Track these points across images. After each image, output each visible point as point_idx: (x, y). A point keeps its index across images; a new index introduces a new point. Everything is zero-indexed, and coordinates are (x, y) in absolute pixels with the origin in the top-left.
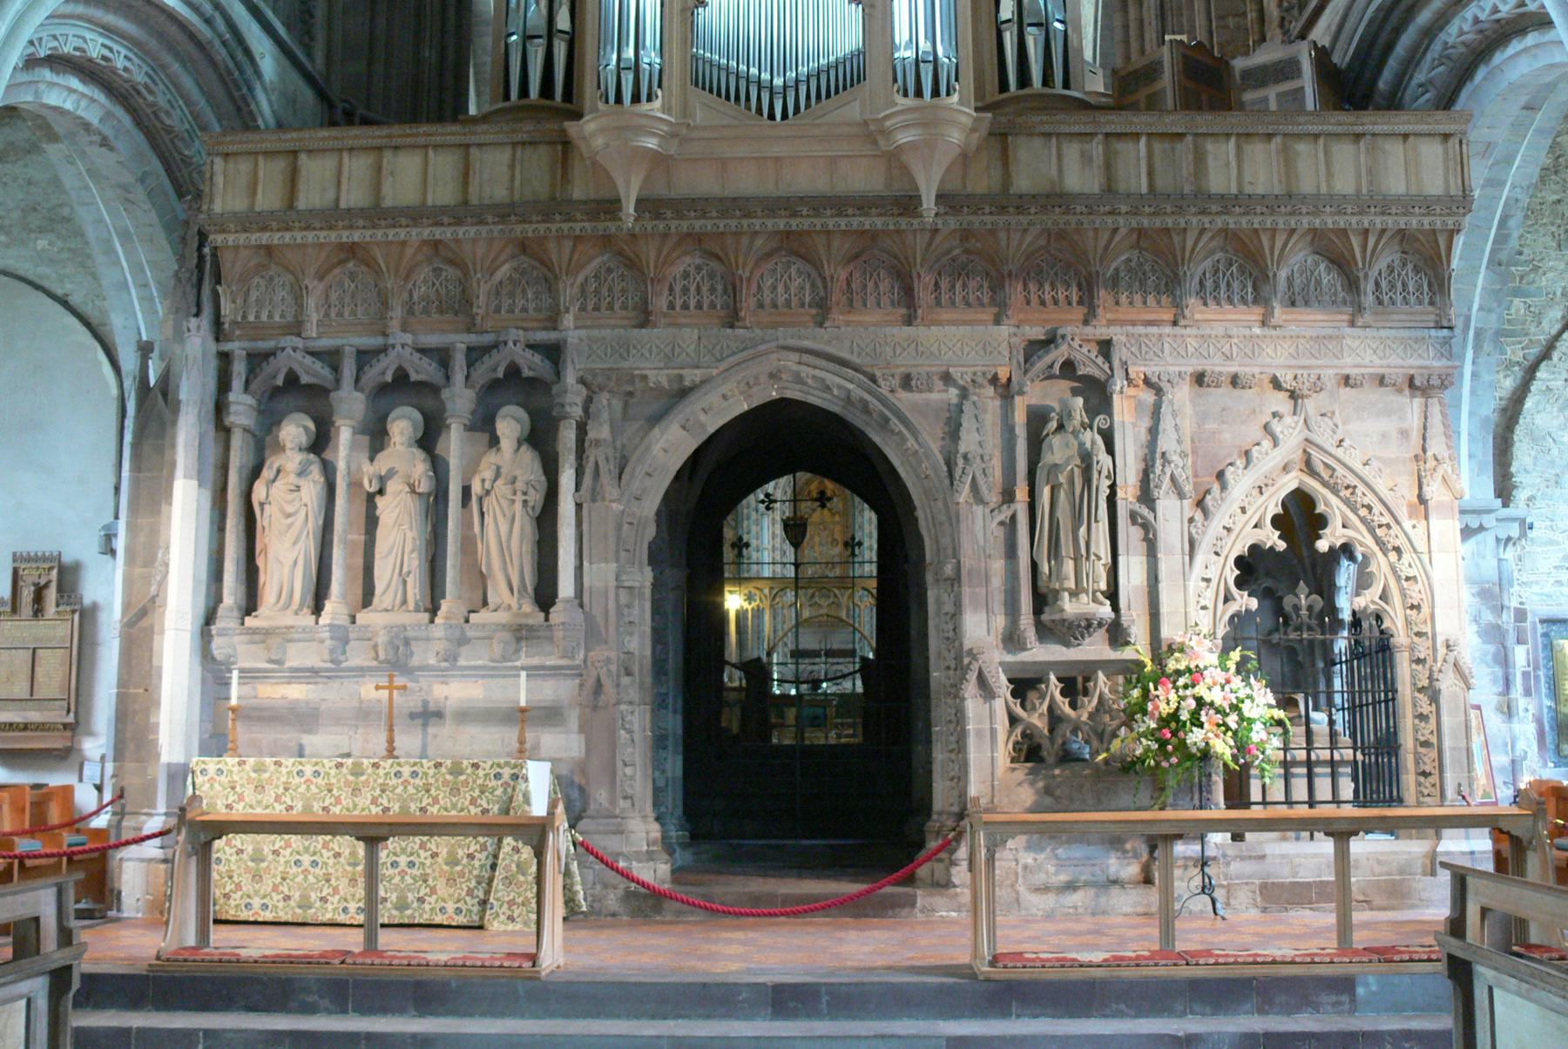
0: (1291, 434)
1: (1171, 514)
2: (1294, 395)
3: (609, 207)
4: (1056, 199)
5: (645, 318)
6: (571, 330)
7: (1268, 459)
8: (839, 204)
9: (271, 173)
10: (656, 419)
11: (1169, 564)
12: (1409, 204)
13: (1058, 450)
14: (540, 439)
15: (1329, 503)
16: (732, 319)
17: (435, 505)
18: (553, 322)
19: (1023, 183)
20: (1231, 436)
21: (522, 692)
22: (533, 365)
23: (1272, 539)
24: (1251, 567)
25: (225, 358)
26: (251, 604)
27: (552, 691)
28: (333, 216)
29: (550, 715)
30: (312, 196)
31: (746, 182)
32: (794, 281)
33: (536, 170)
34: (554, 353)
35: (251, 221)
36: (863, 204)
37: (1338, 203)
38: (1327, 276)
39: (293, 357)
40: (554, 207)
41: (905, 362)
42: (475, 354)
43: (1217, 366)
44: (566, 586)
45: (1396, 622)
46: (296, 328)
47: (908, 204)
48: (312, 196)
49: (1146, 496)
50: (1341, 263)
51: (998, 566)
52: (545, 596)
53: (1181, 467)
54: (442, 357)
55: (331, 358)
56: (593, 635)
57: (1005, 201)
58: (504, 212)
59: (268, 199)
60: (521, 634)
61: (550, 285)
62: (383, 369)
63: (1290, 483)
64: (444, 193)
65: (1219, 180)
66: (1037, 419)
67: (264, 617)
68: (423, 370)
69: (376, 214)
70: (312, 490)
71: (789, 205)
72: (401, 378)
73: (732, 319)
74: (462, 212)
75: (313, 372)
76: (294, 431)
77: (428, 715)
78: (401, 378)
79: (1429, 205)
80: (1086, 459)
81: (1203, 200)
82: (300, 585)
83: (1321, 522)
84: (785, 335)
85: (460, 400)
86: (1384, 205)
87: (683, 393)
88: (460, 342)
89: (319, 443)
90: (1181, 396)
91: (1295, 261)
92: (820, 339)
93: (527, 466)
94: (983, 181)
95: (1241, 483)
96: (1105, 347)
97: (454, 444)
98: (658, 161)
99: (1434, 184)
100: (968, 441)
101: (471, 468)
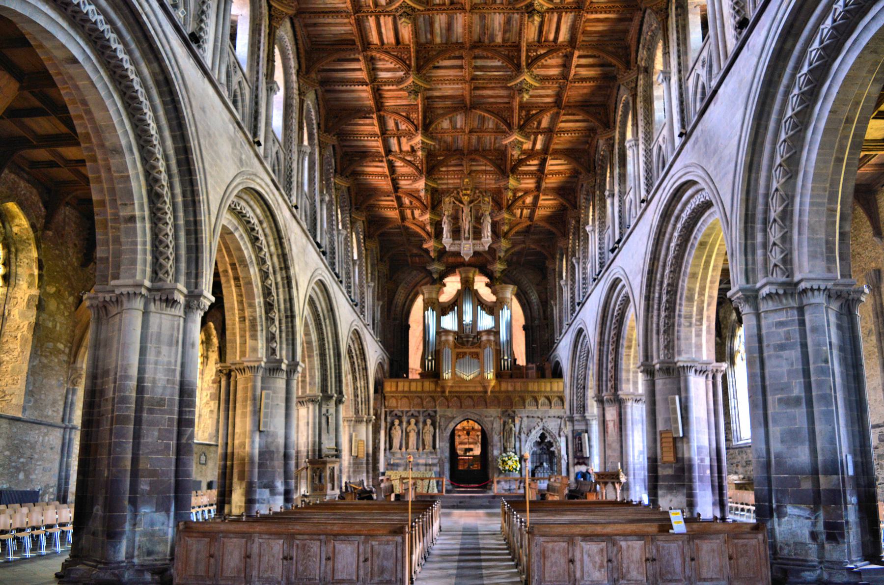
0: (541, 425)
1: (523, 436)
2: (542, 419)
3: (443, 392)
4: (507, 391)
5: (448, 407)
6: (438, 409)
7: (538, 429)
8: (476, 392)
9: (394, 384)
10: (450, 422)
11: (523, 443)
12: (558, 392)
13: (507, 427)
14: (433, 424)
15: (547, 435)
16: (461, 407)
17: (418, 434)
18: (435, 407)
19: (503, 389)
20: (532, 425)
21: (430, 462)
22: (432, 414)
23: (539, 440)
24: (538, 444)
25: (386, 412)
26: (391, 448)
27: (436, 461)
28: (403, 392)
29: (434, 465)
30: (400, 389)
31: (463, 389)
32: (470, 402)
33: (432, 387)
34: (435, 412)
35: (391, 392)
36: (480, 392)
37: (547, 392)
38: (547, 401)
39: (396, 412)
40: (435, 391)
41: (486, 414)
42: (424, 412)
43: (531, 415)
44: (437, 446)
45: (556, 452)
46: (397, 407)
47: (486, 392)
48: (400, 389)
49: (520, 433)
50: (548, 398)
51: (499, 444)
52: (434, 447)
53: (525, 430)
54: (419, 412)
55: (402, 412)
56: (442, 452)
57: (500, 392)
58: (429, 392)
59: (394, 389)
60: (431, 453)
61: (435, 401)
62: (410, 414)
63: (541, 432)
64: (419, 389)
65: (530, 389)
66: (505, 423)
67: (393, 450)
68: (416, 414)
69: (410, 392)
70: (400, 432)
71: (469, 392)
72: (412, 415)
73: (461, 407)
74: (423, 391)
75: (399, 414)
76: (397, 422)
77: (418, 464)
78: (412, 415)
79: (560, 392)
80: (511, 429)
81: (528, 392)
82: (398, 446)
83: (546, 437)
84: (469, 410)
85: (421, 419)
86: (554, 392)
87: (453, 418)
88: (421, 410)
89: (401, 424)
90: (525, 419)
91: (542, 400)
92: (472, 410)
93: (432, 429)
94: (497, 389)
95: (534, 432)
96: (514, 412)
97: (421, 425)
98: (452, 387)
99: (561, 389)
100: (495, 425)
101: (423, 429)
